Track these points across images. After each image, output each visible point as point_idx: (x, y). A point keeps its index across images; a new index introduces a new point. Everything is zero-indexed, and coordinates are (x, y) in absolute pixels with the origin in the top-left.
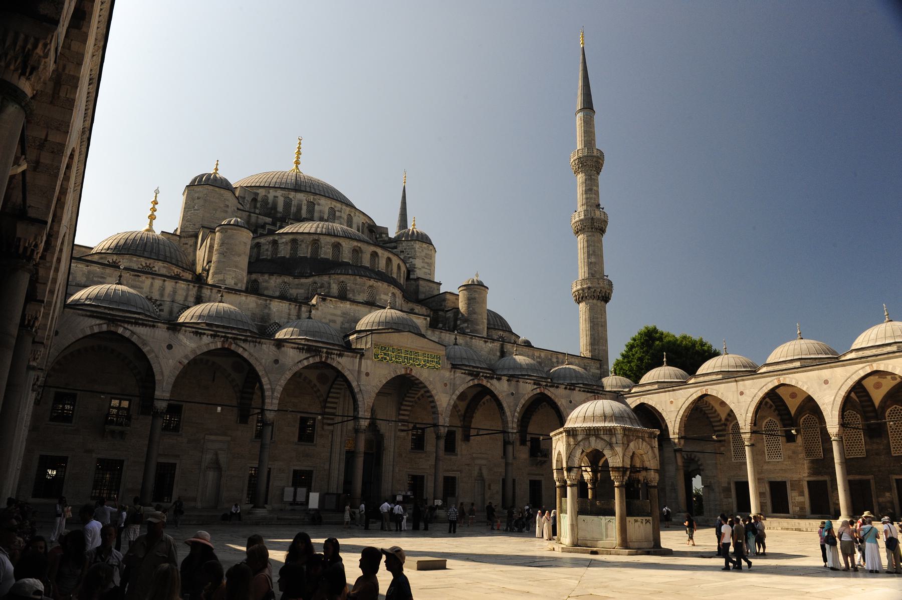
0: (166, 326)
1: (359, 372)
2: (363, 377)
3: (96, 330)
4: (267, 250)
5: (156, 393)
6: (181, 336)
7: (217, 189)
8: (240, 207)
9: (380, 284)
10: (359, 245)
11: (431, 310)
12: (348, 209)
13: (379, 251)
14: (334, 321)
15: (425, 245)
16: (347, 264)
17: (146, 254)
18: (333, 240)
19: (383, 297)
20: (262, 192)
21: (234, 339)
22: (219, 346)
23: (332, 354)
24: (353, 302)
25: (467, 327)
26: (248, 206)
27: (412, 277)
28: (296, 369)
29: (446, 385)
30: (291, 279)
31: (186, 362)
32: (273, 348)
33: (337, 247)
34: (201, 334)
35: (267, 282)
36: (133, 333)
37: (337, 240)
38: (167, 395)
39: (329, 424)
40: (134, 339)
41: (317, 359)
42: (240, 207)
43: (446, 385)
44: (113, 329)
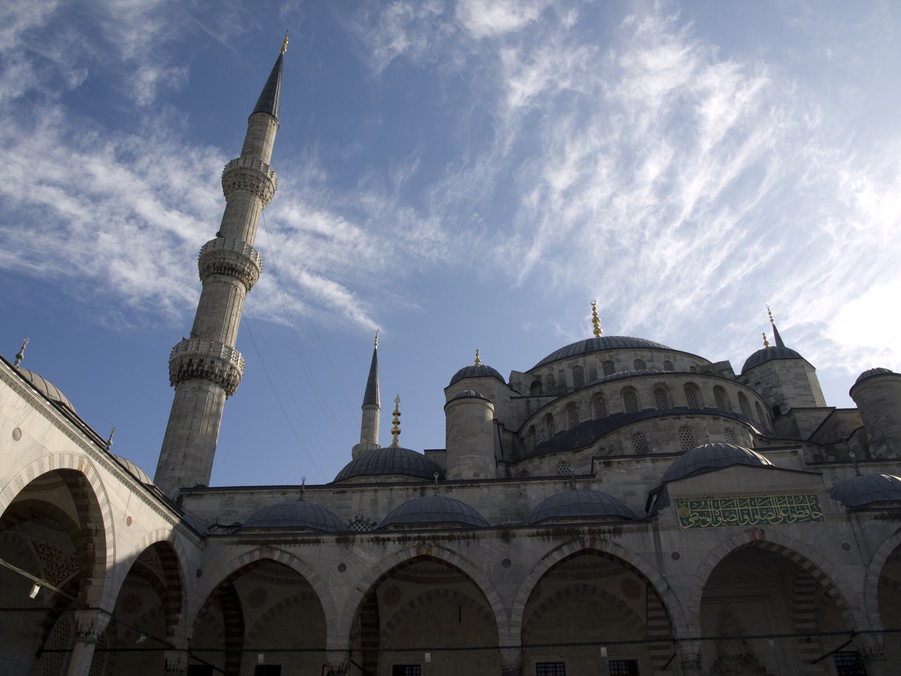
0: (333, 538)
1: (659, 554)
3: (247, 560)
4: (543, 430)
5: (329, 641)
6: (357, 549)
7: (476, 380)
8: (514, 394)
9: (697, 419)
10: (662, 380)
11: (820, 446)
12: (662, 355)
14: (633, 494)
15: (789, 363)
16: (652, 410)
17: (377, 472)
18: (621, 385)
20: (544, 372)
21: (434, 538)
22: (413, 554)
23: (600, 532)
24: (656, 457)
25: (889, 451)
27: (783, 413)
28: (543, 569)
29: (846, 547)
30: (570, 454)
31: (367, 587)
32: (497, 542)
33: (629, 393)
34: (384, 540)
36: (293, 556)
37: (626, 383)
38: (344, 643)
39: (664, 668)
40: (295, 565)
41: (577, 547)
42: (514, 394)
43: (846, 547)
44: (267, 555)
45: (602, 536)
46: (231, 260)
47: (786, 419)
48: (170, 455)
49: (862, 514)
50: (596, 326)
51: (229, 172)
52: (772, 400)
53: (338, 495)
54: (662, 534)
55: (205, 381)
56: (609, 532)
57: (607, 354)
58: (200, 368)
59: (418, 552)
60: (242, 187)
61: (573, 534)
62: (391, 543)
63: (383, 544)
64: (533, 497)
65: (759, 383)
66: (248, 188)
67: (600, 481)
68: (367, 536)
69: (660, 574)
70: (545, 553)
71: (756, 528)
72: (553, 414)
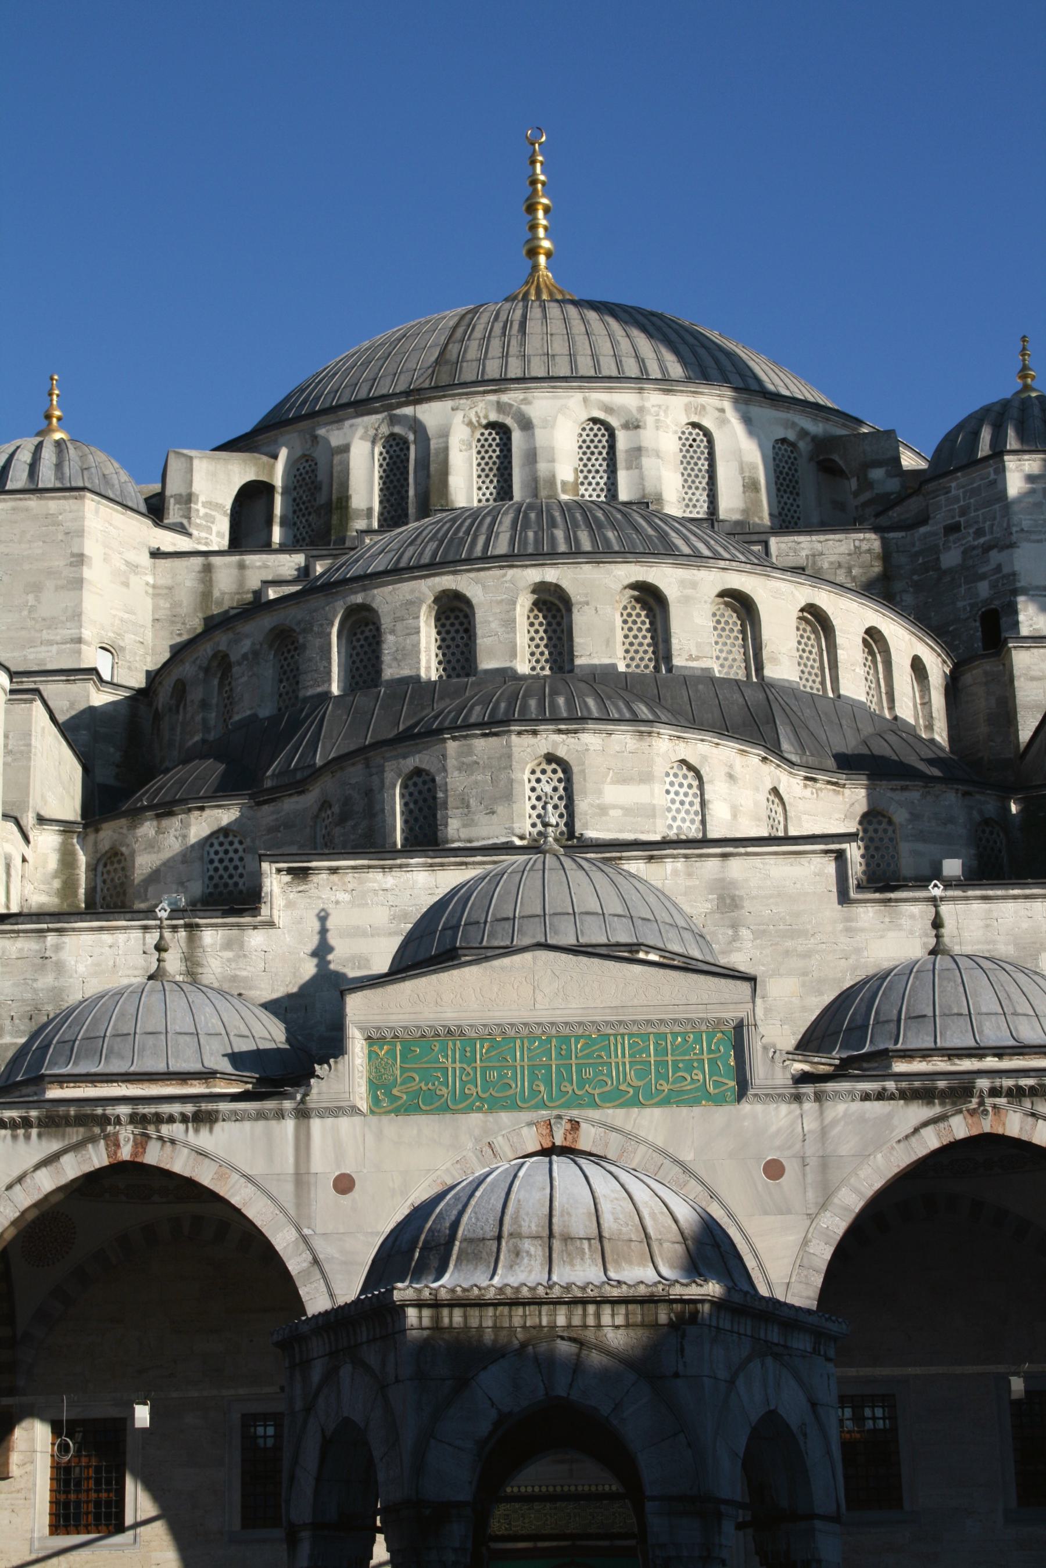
1: (302, 1179)
2: (324, 1194)
4: (204, 705)
7: (33, 503)
10: (551, 574)
13: (665, 576)
16: (507, 675)
19: (614, 794)
23: (159, 1119)
26: (223, 525)
29: (774, 1170)
35: (152, 846)
37: (446, 582)
41: (97, 1157)
42: (169, 541)
43: (774, 1170)
45: (165, 1130)
47: (988, 665)
49: (830, 1086)
50: (533, 227)
52: (983, 589)
54: (316, 1125)
56: (184, 1119)
57: (492, 398)
61: (90, 1119)
64: (81, 969)
65: (953, 529)
67: (270, 924)
69: (299, 1230)
70: (16, 1173)
71: (559, 1117)
72: (233, 658)
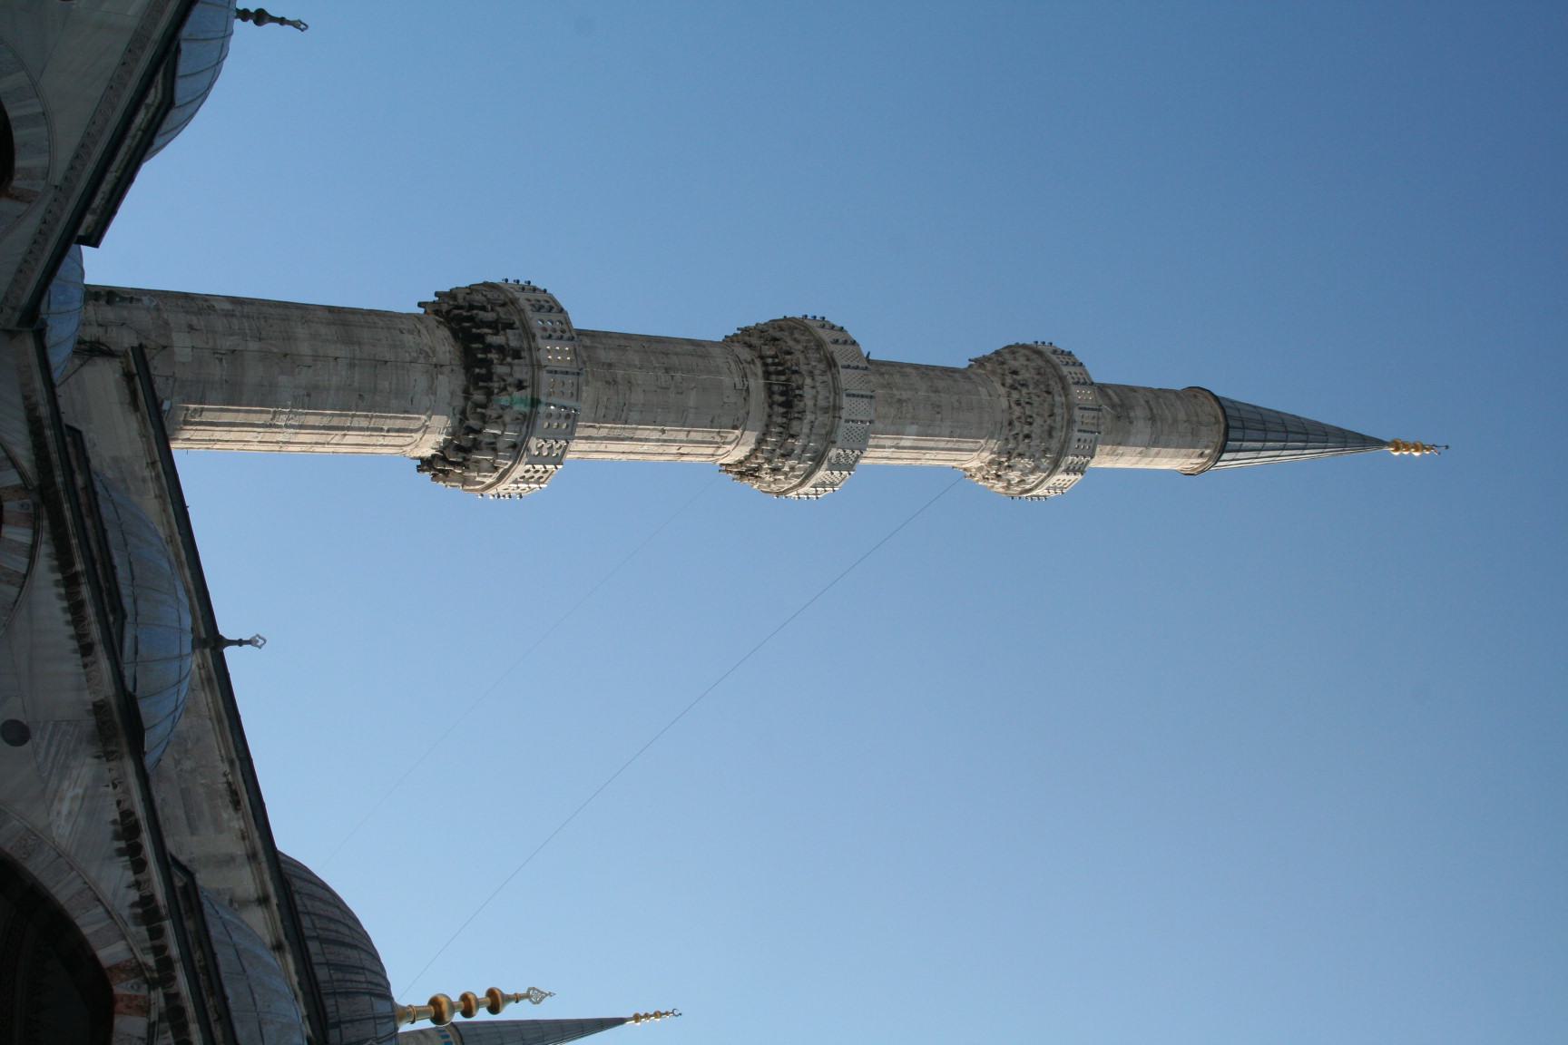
0: (107, 690)
6: (86, 769)
21: (175, 1014)
22: (111, 953)
46: (812, 393)
48: (229, 315)
51: (1039, 353)
53: (222, 787)
55: (459, 380)
58: (493, 356)
59: (117, 968)
60: (1015, 395)
62: (130, 876)
63: (120, 852)
66: (1017, 411)
68: (136, 795)
